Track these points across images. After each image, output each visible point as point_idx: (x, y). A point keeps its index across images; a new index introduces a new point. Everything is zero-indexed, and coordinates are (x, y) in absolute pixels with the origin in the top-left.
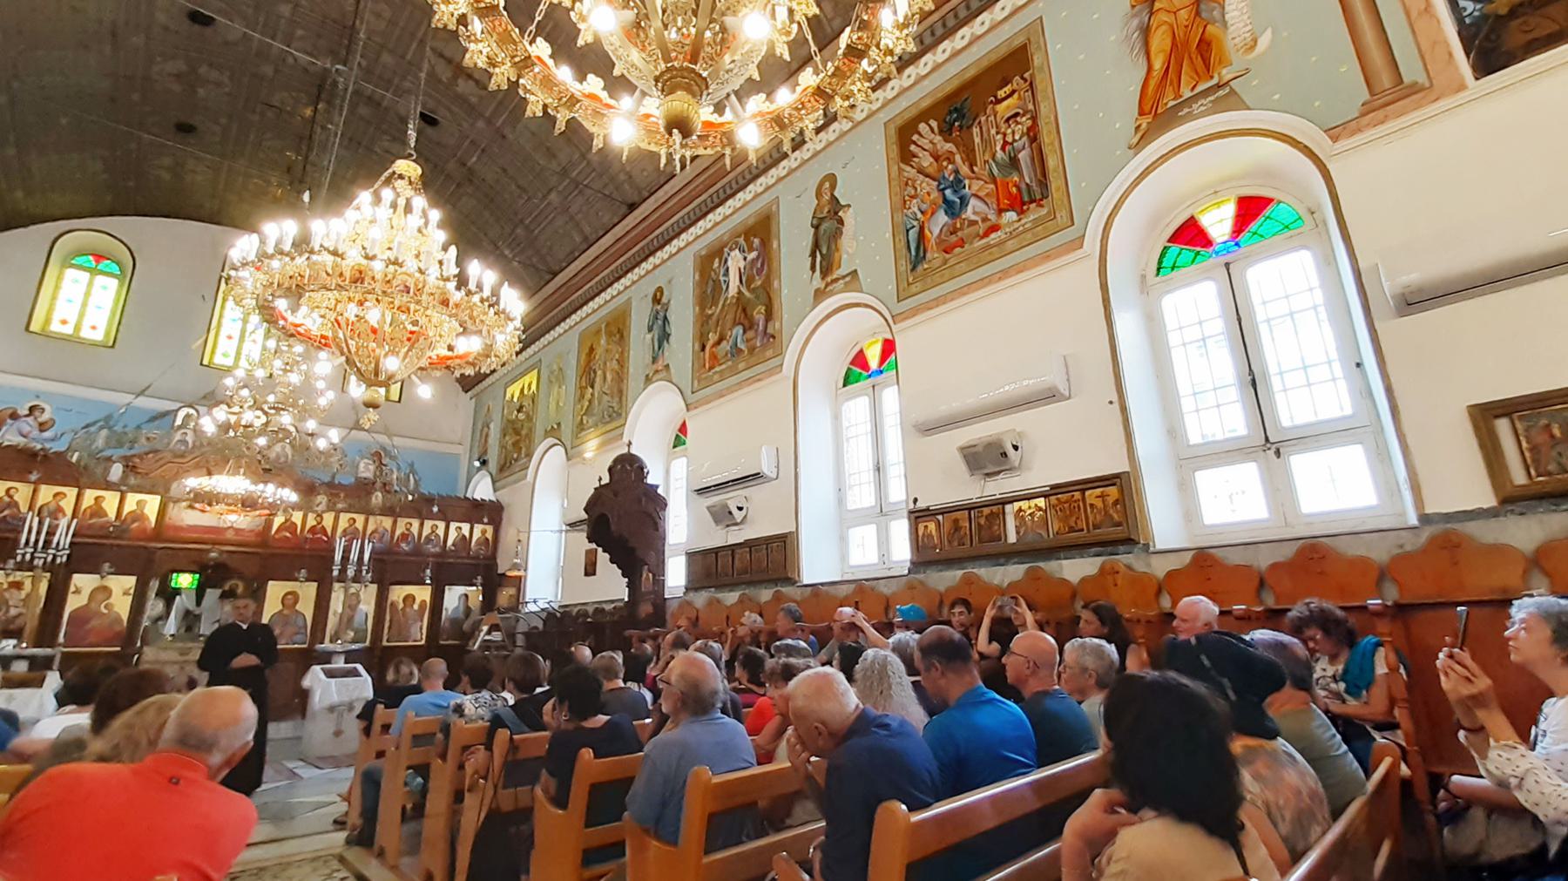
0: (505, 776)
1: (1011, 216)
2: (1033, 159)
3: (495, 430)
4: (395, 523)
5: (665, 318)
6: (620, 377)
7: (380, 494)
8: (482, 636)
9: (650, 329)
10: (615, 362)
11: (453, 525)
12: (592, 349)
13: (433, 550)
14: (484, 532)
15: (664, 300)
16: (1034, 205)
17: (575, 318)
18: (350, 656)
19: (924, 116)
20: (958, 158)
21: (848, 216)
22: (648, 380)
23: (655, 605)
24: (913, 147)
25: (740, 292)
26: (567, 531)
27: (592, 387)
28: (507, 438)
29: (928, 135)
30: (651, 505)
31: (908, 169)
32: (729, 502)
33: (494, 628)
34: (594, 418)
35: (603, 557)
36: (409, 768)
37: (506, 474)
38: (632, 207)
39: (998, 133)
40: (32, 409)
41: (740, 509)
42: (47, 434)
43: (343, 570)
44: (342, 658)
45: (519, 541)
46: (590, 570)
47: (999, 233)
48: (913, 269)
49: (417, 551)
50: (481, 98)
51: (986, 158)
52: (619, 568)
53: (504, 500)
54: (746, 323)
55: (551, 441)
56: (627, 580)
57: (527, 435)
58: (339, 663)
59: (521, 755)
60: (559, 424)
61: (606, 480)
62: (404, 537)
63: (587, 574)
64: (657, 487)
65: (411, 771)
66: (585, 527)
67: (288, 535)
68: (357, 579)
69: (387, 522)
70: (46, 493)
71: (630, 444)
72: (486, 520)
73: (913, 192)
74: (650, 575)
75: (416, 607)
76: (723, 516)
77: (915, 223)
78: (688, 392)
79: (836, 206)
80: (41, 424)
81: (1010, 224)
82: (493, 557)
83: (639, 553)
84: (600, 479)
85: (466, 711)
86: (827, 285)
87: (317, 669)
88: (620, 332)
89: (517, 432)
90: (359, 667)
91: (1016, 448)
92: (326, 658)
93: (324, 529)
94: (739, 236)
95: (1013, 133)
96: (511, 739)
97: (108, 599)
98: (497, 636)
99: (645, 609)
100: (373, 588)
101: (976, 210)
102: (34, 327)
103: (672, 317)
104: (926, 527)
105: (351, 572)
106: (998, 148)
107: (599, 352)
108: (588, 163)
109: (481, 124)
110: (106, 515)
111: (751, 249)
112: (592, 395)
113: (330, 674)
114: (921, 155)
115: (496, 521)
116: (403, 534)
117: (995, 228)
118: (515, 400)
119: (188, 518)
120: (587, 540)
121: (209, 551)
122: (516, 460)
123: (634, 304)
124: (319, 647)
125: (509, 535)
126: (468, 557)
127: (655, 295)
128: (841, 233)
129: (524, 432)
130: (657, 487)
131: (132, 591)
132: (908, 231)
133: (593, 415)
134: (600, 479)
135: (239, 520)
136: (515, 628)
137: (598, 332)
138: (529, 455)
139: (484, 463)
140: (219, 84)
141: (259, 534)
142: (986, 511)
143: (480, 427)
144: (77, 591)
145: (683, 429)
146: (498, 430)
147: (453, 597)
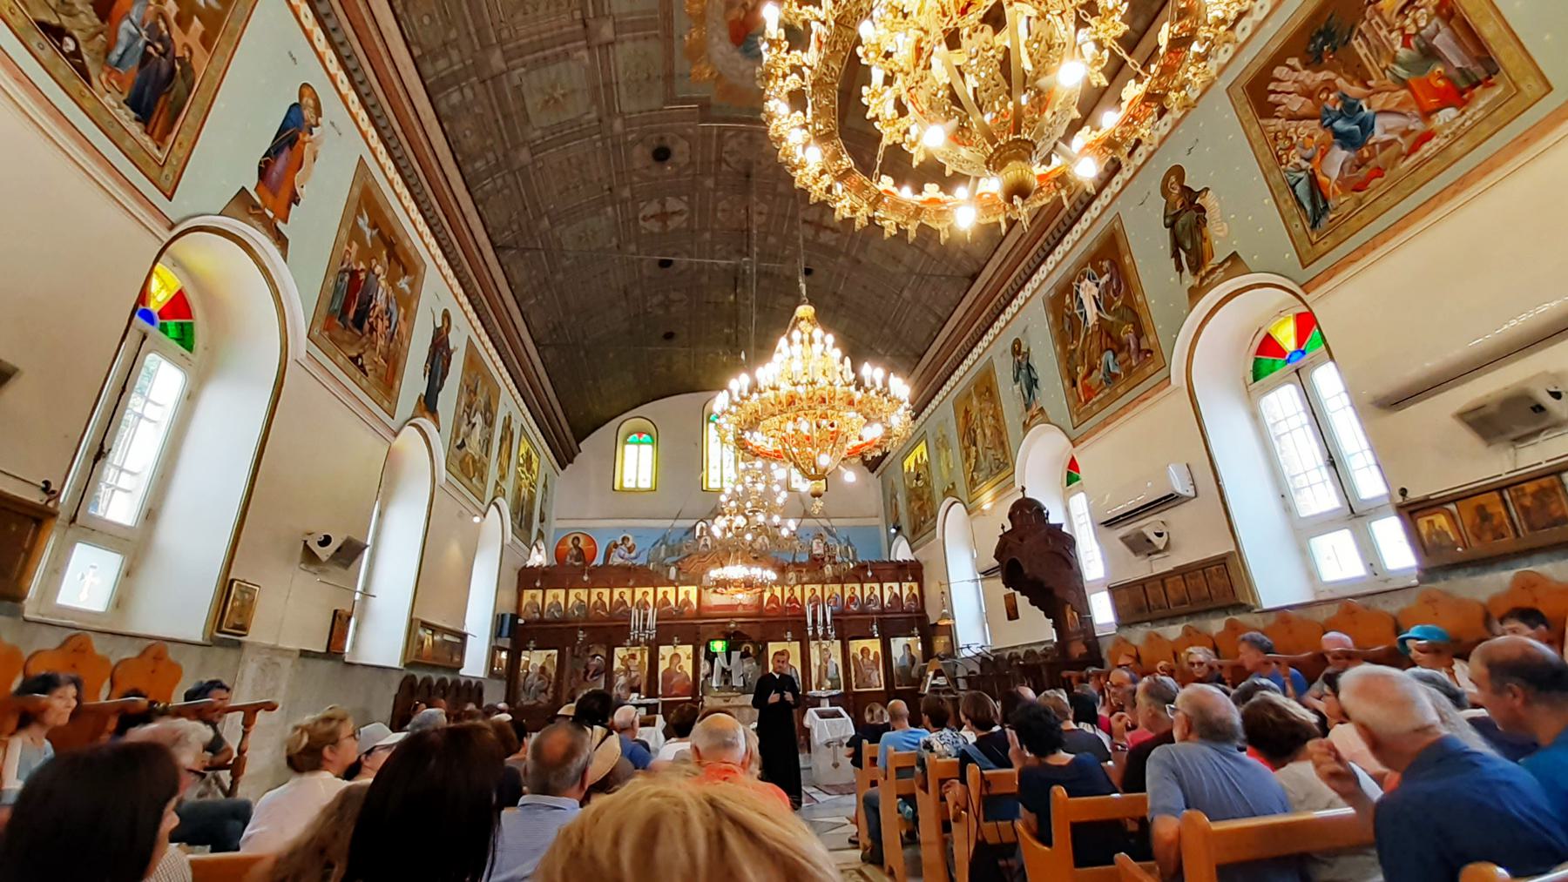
0: (984, 809)
1: (1449, 113)
2: (1457, 39)
3: (901, 499)
4: (843, 588)
5: (1028, 365)
6: (999, 431)
7: (829, 566)
8: (930, 681)
9: (1016, 380)
10: (990, 418)
11: (886, 586)
12: (967, 412)
14: (911, 589)
15: (1024, 349)
16: (1479, 88)
17: (946, 388)
18: (833, 700)
19: (1278, 59)
20: (1340, 82)
21: (1209, 202)
22: (1026, 427)
23: (1088, 646)
24: (1272, 98)
25: (1100, 319)
26: (982, 579)
27: (975, 445)
28: (913, 504)
29: (1292, 78)
30: (1061, 545)
31: (1274, 121)
32: (1144, 530)
33: (938, 673)
34: (983, 473)
35: (1022, 601)
36: (898, 797)
37: (919, 535)
38: (974, 278)
39: (1391, 32)
40: (624, 539)
41: (1160, 535)
42: (633, 555)
43: (815, 631)
44: (827, 701)
45: (943, 593)
46: (1013, 614)
47: (1435, 140)
48: (1313, 227)
49: (863, 611)
50: (837, 239)
51: (1383, 65)
52: (1041, 609)
53: (922, 560)
54: (1115, 347)
55: (950, 500)
56: (1051, 620)
57: (928, 498)
58: (826, 706)
59: (995, 790)
60: (953, 484)
61: (1009, 527)
62: (852, 599)
63: (1010, 618)
64: (1061, 525)
65: (900, 800)
66: (999, 573)
68: (825, 637)
69: (837, 588)
70: (639, 592)
71: (1023, 489)
72: (910, 578)
73: (1287, 143)
74: (1075, 614)
75: (871, 658)
76: (1140, 545)
77: (1301, 175)
78: (1069, 428)
79: (1190, 196)
80: (629, 548)
81: (1447, 125)
82: (923, 610)
83: (1058, 593)
84: (1003, 527)
85: (935, 748)
86: (1202, 280)
87: (811, 711)
88: (989, 390)
89: (920, 498)
90: (840, 709)
91: (1557, 395)
92: (816, 702)
93: (795, 598)
94: (1086, 266)
95: (1415, 21)
96: (982, 775)
98: (942, 681)
99: (1078, 649)
100: (838, 642)
101: (1388, 127)
102: (617, 487)
103: (1035, 363)
104: (1431, 522)
105: (820, 632)
106: (1398, 47)
107: (974, 413)
108: (929, 255)
109: (841, 259)
110: (670, 604)
111: (1101, 275)
112: (977, 451)
113: (822, 715)
114: (1285, 101)
115: (918, 578)
116: (850, 597)
117: (1427, 137)
118: (912, 470)
119: (715, 599)
120: (1003, 586)
121: (728, 623)
122: (924, 522)
123: (995, 361)
124: (809, 693)
125: (932, 590)
126: (903, 612)
127: (1013, 348)
128: (1205, 221)
129: (925, 497)
130: (1061, 525)
132: (1293, 187)
133: (982, 470)
134: (1003, 527)
135: (743, 597)
136: (955, 674)
137: (969, 396)
138: (934, 516)
139: (899, 529)
140: (681, 301)
141: (757, 607)
142: (1530, 487)
143: (889, 498)
145: (1073, 465)
146: (904, 501)
147: (898, 646)
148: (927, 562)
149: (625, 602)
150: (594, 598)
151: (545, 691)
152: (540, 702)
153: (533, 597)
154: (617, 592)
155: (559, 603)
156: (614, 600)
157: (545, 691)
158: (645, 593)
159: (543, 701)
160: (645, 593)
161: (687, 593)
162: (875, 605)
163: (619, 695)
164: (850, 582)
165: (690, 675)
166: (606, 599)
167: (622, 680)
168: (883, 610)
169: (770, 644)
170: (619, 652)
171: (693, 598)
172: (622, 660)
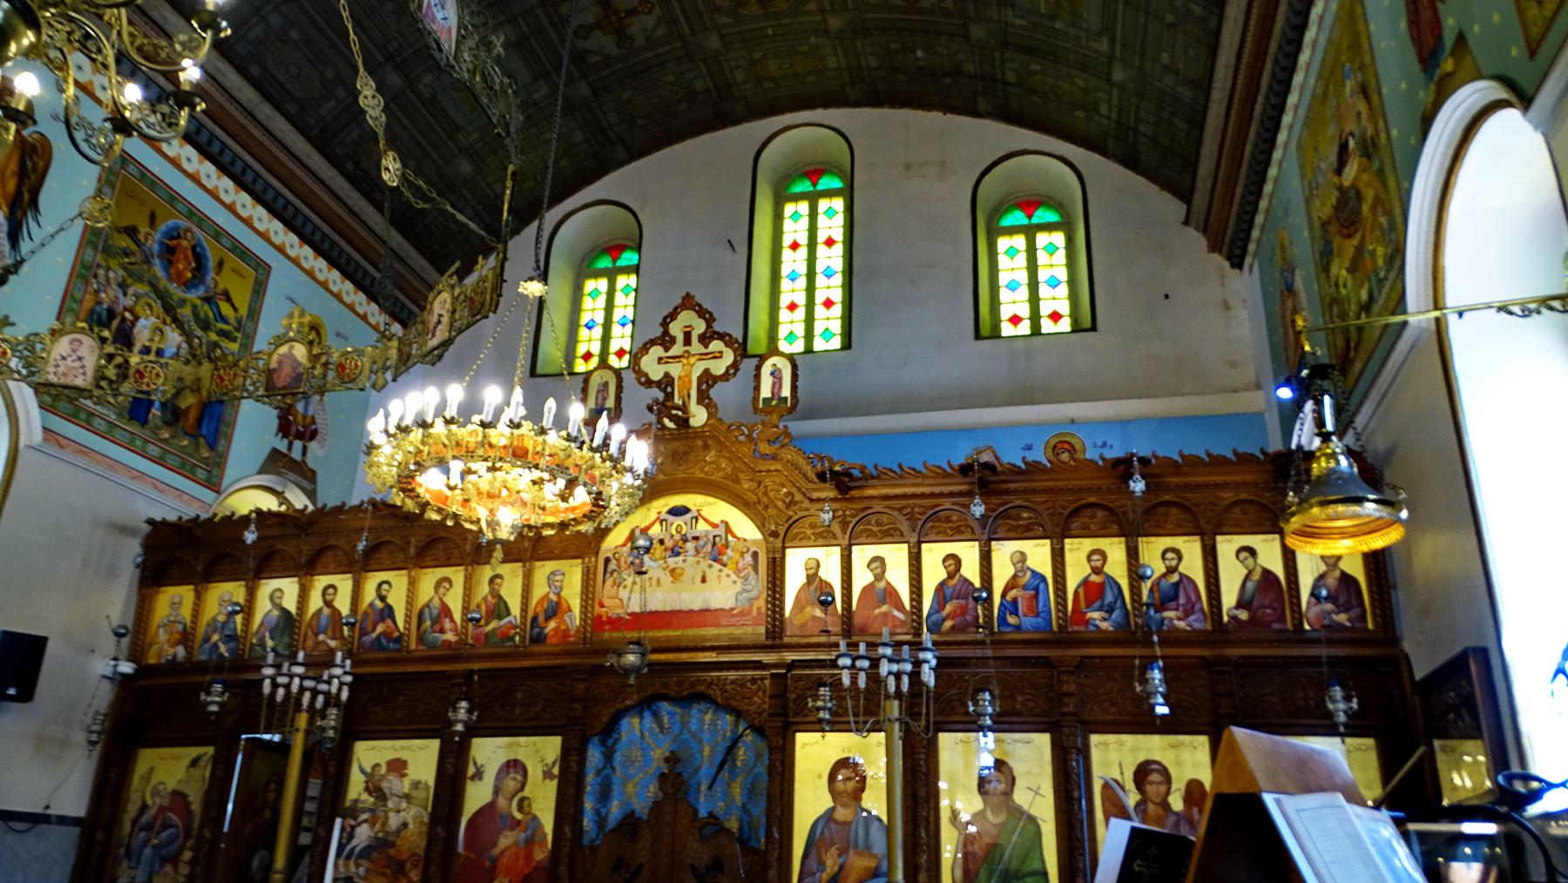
11: (1227, 546)
13: (1181, 624)
37: (1357, 367)
62: (1094, 591)
75: (1176, 803)
97: (522, 788)
110: (508, 613)
116: (1085, 583)
131: (556, 771)
148: (1389, 454)
149: (390, 608)
150: (315, 602)
157: (174, 860)
162: (1187, 614)
164: (1087, 533)
165: (548, 823)
166: (343, 605)
168: (1220, 631)
169: (801, 738)
171: (573, 596)
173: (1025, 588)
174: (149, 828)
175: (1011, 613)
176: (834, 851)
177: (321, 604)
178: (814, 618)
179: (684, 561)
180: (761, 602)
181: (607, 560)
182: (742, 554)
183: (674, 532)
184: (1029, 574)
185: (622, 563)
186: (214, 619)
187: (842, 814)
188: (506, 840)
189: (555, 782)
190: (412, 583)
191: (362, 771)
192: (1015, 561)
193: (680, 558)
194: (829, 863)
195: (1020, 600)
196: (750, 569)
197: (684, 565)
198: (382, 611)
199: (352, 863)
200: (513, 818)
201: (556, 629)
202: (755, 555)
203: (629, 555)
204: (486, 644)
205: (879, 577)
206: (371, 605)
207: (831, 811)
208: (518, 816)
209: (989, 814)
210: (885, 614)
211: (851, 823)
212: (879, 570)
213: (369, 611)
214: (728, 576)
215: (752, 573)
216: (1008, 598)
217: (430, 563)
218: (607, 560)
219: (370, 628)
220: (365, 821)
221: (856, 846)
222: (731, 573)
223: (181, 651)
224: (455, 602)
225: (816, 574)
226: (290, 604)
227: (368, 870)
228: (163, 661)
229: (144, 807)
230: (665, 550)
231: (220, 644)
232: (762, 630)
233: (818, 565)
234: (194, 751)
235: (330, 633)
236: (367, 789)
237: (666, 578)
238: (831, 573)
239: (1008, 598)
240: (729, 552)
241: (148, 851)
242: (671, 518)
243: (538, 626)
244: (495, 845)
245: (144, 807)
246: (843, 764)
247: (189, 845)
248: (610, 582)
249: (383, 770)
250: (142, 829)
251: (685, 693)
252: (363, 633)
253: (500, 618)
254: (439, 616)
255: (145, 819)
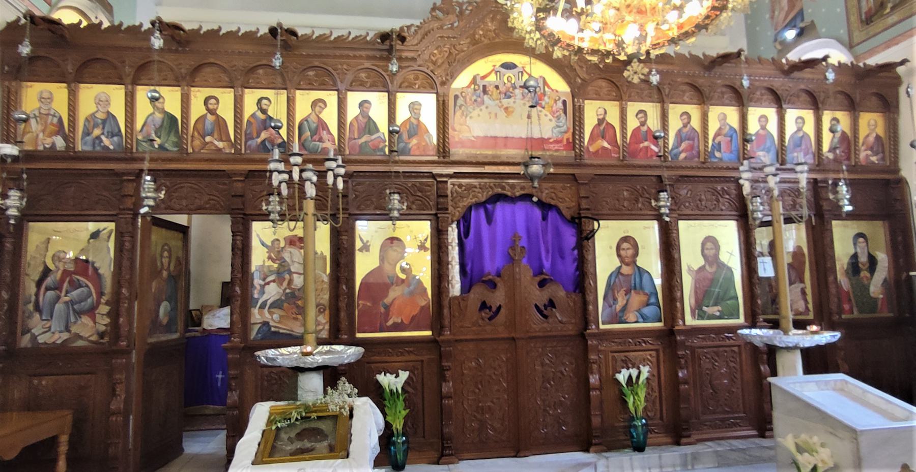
67: (606, 145)
70: (304, 100)
110: (377, 130)
131: (428, 244)
144: (366, 248)
150: (197, 109)
151: (91, 312)
152: (78, 337)
153: (46, 99)
154: (251, 98)
155: (111, 117)
156: (247, 115)
157: (91, 312)
158: (318, 104)
159: (85, 333)
160: (318, 104)
161: (414, 108)
163: (266, 324)
166: (226, 112)
167: (273, 292)
170: (261, 231)
172: (270, 249)
173: (725, 136)
174: (57, 287)
175: (718, 151)
176: (622, 292)
177: (203, 111)
178: (604, 148)
179: (514, 102)
180: (569, 135)
181: (456, 97)
182: (556, 101)
183: (506, 82)
184: (728, 127)
185: (468, 100)
186: (93, 115)
187: (626, 270)
188: (394, 293)
189: (429, 252)
190: (291, 102)
191: (263, 244)
192: (721, 118)
193: (511, 100)
194: (620, 299)
195: (722, 143)
196: (561, 112)
197: (514, 106)
198: (264, 121)
199: (266, 310)
200: (398, 277)
201: (418, 145)
202: (564, 102)
203: (473, 95)
204: (360, 153)
205: (643, 124)
206: (253, 115)
207: (620, 268)
208: (403, 276)
209: (707, 267)
210: (647, 148)
211: (631, 275)
212: (643, 119)
213: (252, 120)
214: (546, 115)
215: (563, 115)
216: (716, 141)
217: (304, 87)
218: (456, 97)
219: (255, 135)
220: (274, 281)
221: (635, 288)
222: (548, 114)
223: (60, 143)
224: (330, 116)
225: (604, 119)
226: (174, 108)
227: (281, 317)
228: (41, 148)
229: (46, 272)
230: (500, 93)
231: (103, 138)
232: (572, 154)
233: (606, 113)
234: (92, 226)
235: (216, 135)
236: (270, 258)
237: (502, 114)
238: (613, 118)
239: (716, 141)
240: (546, 98)
241: (59, 307)
242: (503, 70)
243: (403, 142)
244: (386, 296)
245: (46, 272)
246: (626, 239)
247: (103, 301)
248: (458, 113)
249: (282, 244)
250: (47, 289)
251: (518, 194)
252: (249, 137)
253: (370, 133)
254: (317, 129)
255: (49, 281)
